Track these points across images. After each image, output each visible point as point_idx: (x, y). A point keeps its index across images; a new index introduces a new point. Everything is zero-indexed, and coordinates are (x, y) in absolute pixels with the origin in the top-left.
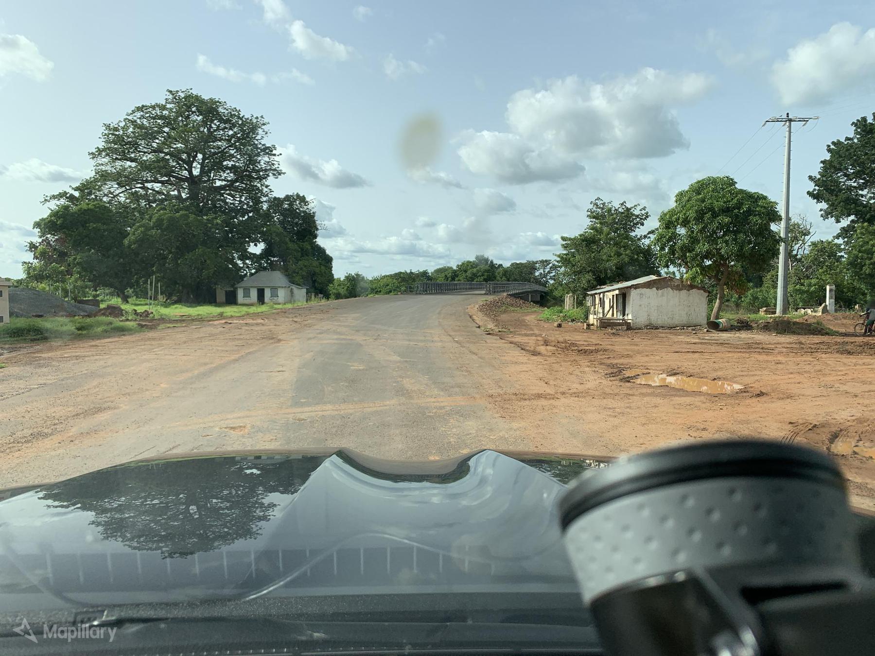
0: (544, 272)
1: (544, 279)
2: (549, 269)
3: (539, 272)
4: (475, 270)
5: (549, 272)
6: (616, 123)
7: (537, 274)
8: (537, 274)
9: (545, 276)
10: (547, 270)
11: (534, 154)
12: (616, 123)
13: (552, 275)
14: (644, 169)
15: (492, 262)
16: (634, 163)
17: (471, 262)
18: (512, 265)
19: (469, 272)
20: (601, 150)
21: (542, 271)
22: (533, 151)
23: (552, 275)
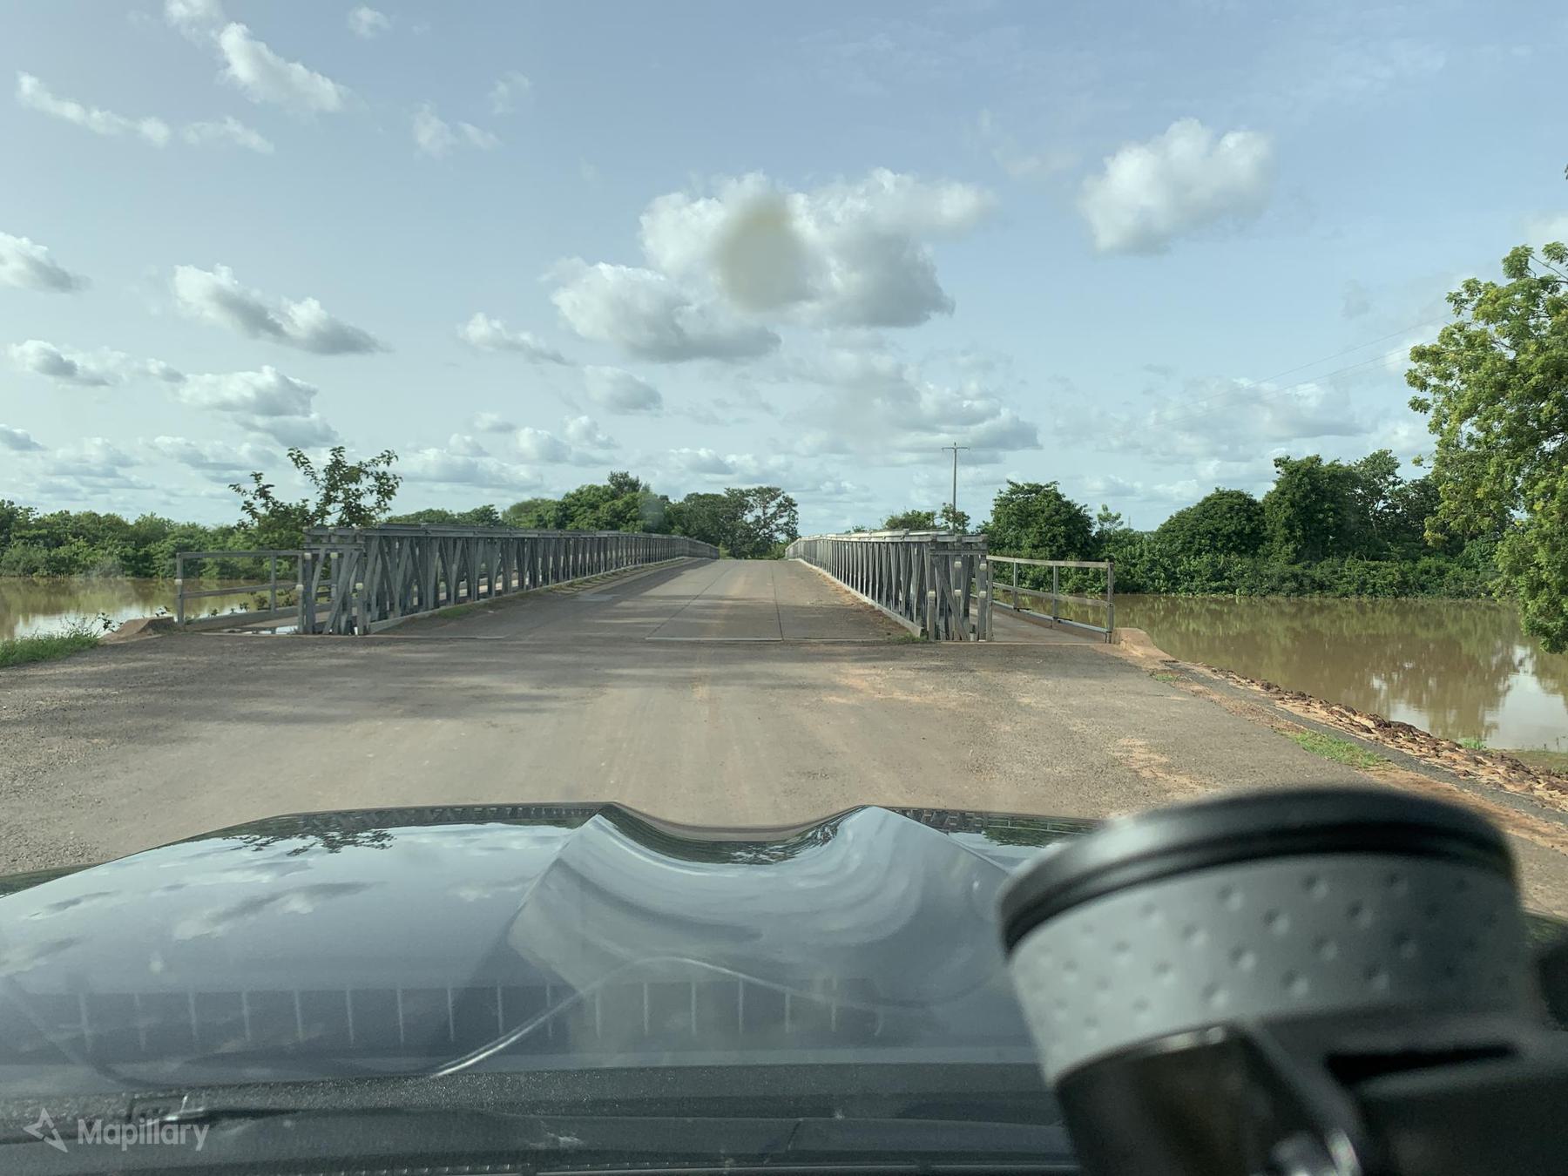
0: (765, 514)
1: (767, 531)
3: (754, 514)
4: (619, 503)
5: (774, 516)
6: (833, 262)
7: (749, 518)
8: (749, 518)
9: (766, 525)
10: (770, 511)
11: (693, 308)
12: (833, 262)
13: (781, 521)
14: (879, 346)
15: (647, 489)
16: (862, 334)
17: (598, 489)
18: (689, 498)
19: (604, 508)
20: (808, 309)
22: (688, 304)
23: (781, 521)
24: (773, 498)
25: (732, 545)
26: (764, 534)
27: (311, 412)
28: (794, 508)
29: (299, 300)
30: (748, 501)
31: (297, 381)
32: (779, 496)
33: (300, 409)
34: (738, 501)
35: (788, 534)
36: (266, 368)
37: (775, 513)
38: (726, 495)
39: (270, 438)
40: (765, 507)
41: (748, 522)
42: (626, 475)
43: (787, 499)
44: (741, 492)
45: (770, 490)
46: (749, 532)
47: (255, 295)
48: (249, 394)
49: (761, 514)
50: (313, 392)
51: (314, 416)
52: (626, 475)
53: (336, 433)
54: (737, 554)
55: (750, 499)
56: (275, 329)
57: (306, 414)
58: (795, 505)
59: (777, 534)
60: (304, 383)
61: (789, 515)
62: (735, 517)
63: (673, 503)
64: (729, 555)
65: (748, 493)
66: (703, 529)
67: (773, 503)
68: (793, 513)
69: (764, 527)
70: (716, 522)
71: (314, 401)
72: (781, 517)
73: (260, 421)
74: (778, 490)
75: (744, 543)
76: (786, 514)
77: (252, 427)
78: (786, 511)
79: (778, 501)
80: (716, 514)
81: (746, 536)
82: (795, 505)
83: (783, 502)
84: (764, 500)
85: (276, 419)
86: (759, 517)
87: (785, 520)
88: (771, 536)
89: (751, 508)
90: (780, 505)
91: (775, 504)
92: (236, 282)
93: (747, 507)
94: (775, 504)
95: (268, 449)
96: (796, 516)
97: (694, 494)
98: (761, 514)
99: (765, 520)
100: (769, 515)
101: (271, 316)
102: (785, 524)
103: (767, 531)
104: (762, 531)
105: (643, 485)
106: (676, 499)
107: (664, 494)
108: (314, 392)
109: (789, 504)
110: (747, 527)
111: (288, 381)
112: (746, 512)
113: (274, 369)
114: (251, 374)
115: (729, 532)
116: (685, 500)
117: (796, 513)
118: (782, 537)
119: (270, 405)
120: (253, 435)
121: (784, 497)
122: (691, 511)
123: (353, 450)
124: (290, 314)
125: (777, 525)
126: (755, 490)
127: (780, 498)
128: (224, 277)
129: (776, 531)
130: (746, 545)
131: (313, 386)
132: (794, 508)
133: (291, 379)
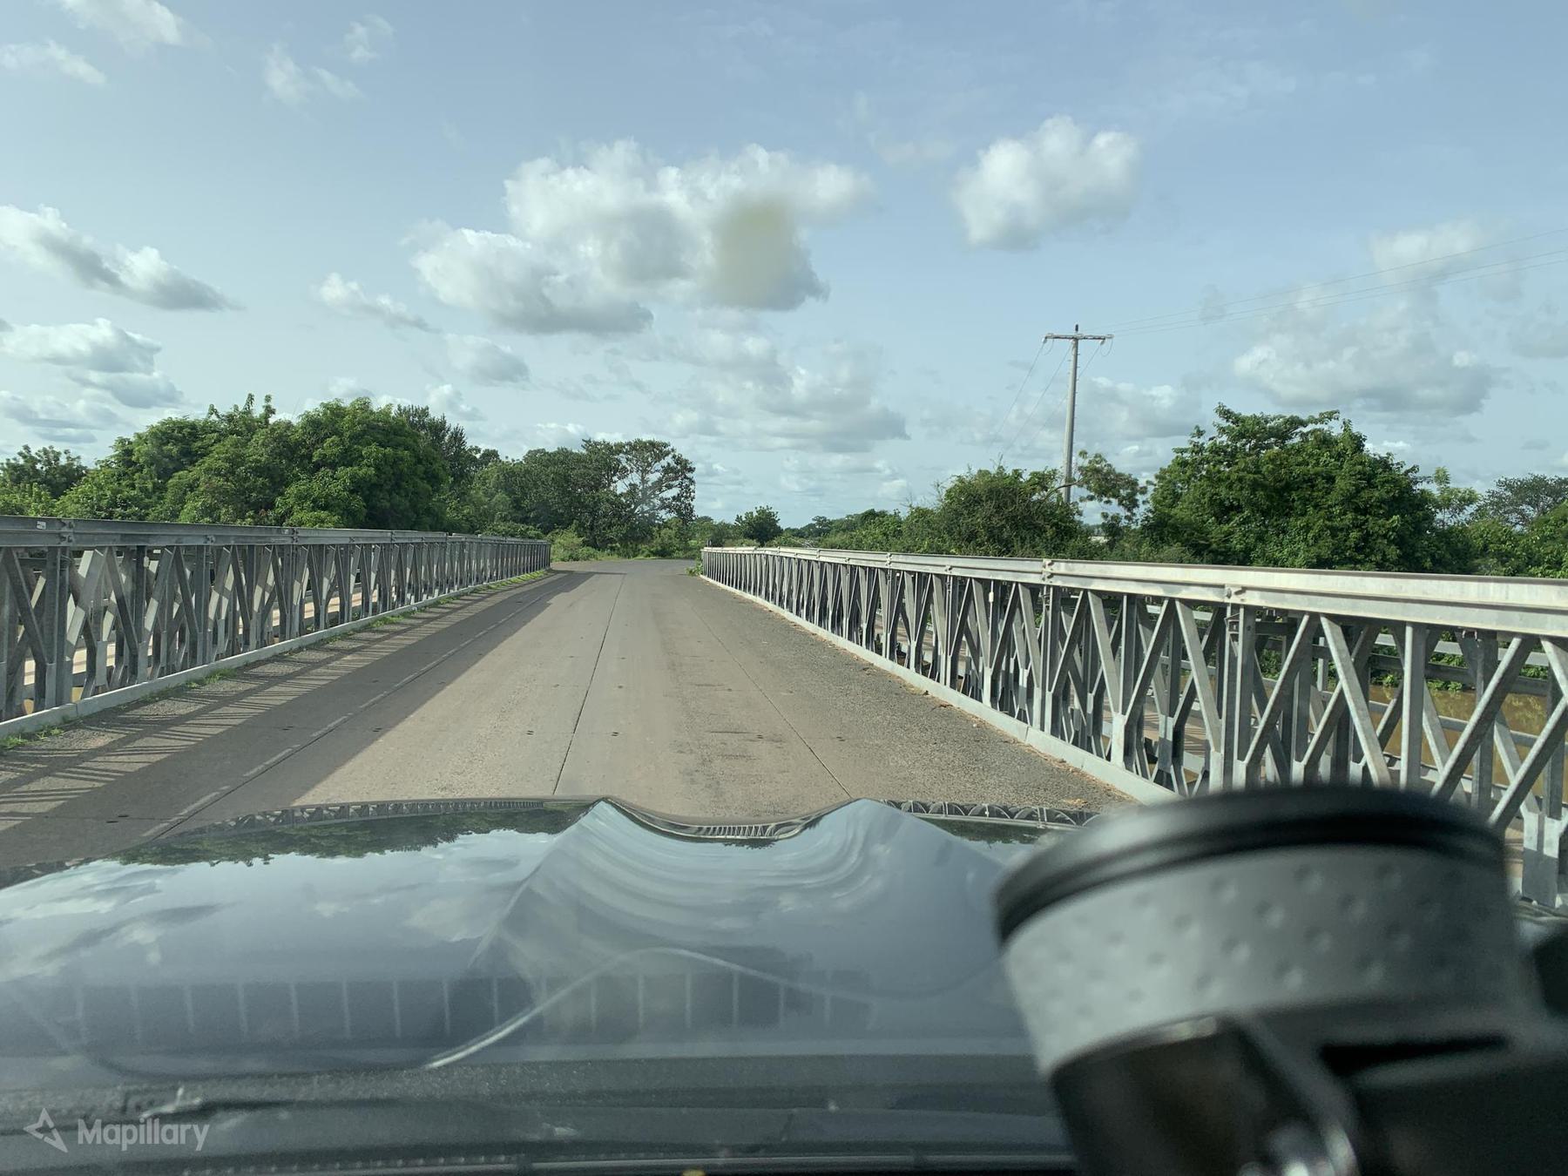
0: (644, 481)
1: (646, 508)
2: (658, 475)
3: (627, 481)
5: (658, 485)
7: (621, 487)
8: (621, 487)
10: (653, 477)
13: (670, 494)
21: (635, 478)
23: (670, 494)
24: (658, 458)
25: (592, 528)
26: (643, 512)
27: (153, 371)
28: (689, 475)
29: (136, 250)
30: (619, 461)
31: (137, 337)
32: (667, 454)
33: (139, 363)
34: (603, 460)
35: (678, 511)
36: (101, 321)
37: (660, 480)
38: (584, 452)
39: (108, 395)
40: (645, 471)
41: (618, 493)
42: (425, 412)
43: (678, 460)
44: (608, 446)
45: (652, 444)
46: (620, 510)
47: (87, 242)
48: (83, 347)
49: (638, 482)
50: (158, 349)
51: (156, 374)
52: (425, 412)
53: (181, 393)
54: (597, 542)
55: (622, 457)
56: (111, 279)
57: (149, 372)
58: (691, 470)
59: (664, 515)
60: (149, 340)
61: (680, 485)
62: (597, 486)
63: (504, 460)
64: (585, 543)
65: (619, 448)
66: (545, 503)
67: (658, 466)
68: (687, 482)
69: (642, 501)
70: (565, 493)
71: (157, 358)
72: (670, 487)
73: (95, 376)
74: (665, 445)
75: (610, 526)
76: (677, 483)
77: (87, 383)
78: (676, 479)
79: (664, 462)
80: (566, 479)
81: (614, 515)
82: (691, 470)
83: (673, 464)
84: (645, 460)
85: (113, 376)
86: (634, 487)
87: (675, 492)
88: (654, 516)
89: (624, 473)
90: (667, 469)
91: (660, 468)
92: (64, 225)
93: (616, 470)
94: (660, 468)
95: (107, 407)
96: (692, 487)
97: (538, 451)
98: (638, 482)
99: (644, 491)
100: (650, 484)
101: (106, 265)
102: (674, 498)
103: (646, 508)
104: (639, 508)
105: (452, 430)
106: (513, 453)
107: (491, 448)
108: (158, 349)
109: (681, 470)
110: (616, 503)
111: (128, 338)
112: (615, 478)
113: (109, 322)
114: (86, 326)
115: (586, 507)
116: (525, 459)
117: (692, 482)
118: (664, 515)
119: (106, 360)
120: (89, 391)
121: (674, 457)
122: (527, 472)
123: (199, 412)
124: (127, 263)
125: (662, 500)
126: (629, 444)
127: (669, 459)
128: (50, 221)
129: (663, 507)
130: (614, 529)
131: (159, 344)
132: (689, 475)
133: (130, 334)
